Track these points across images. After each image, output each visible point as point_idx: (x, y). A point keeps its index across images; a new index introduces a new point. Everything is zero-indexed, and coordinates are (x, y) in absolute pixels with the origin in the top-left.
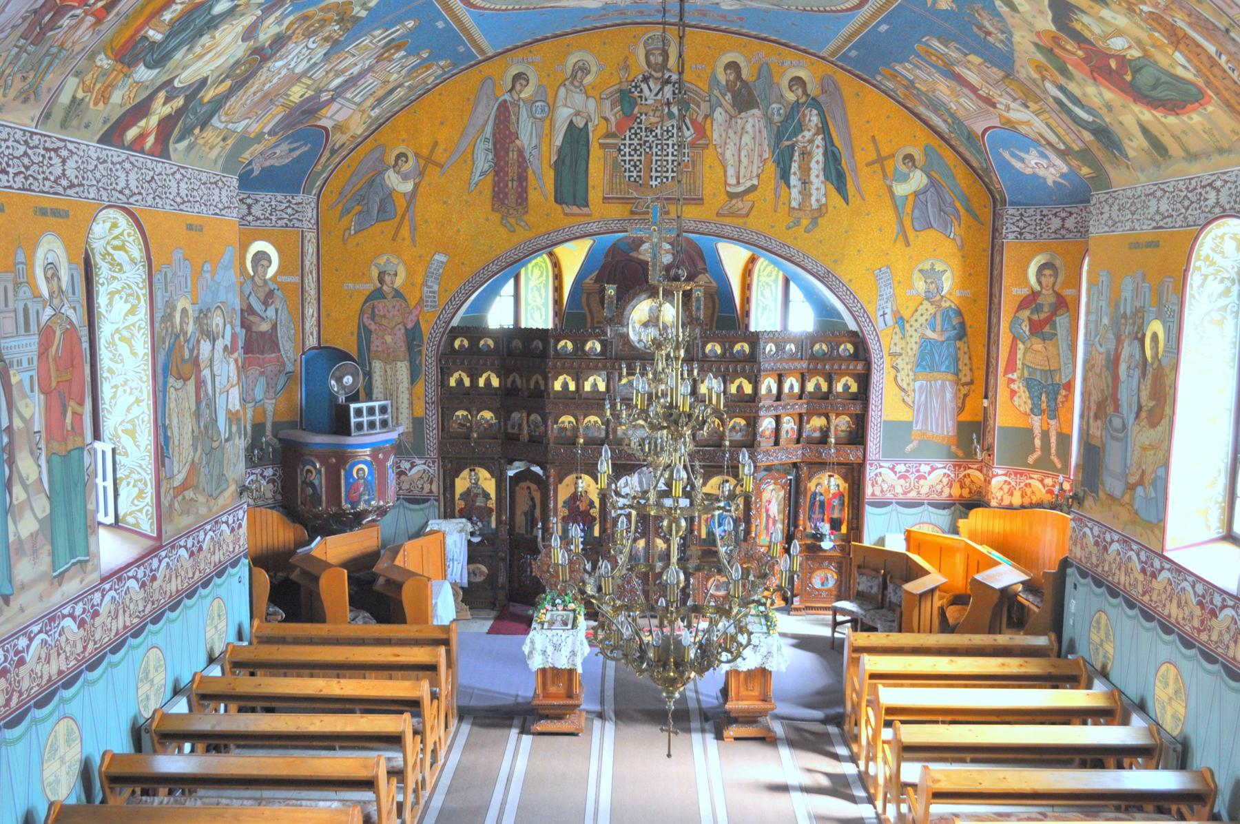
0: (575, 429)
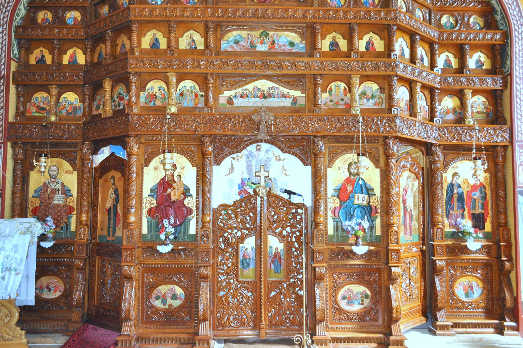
0: (167, 96)
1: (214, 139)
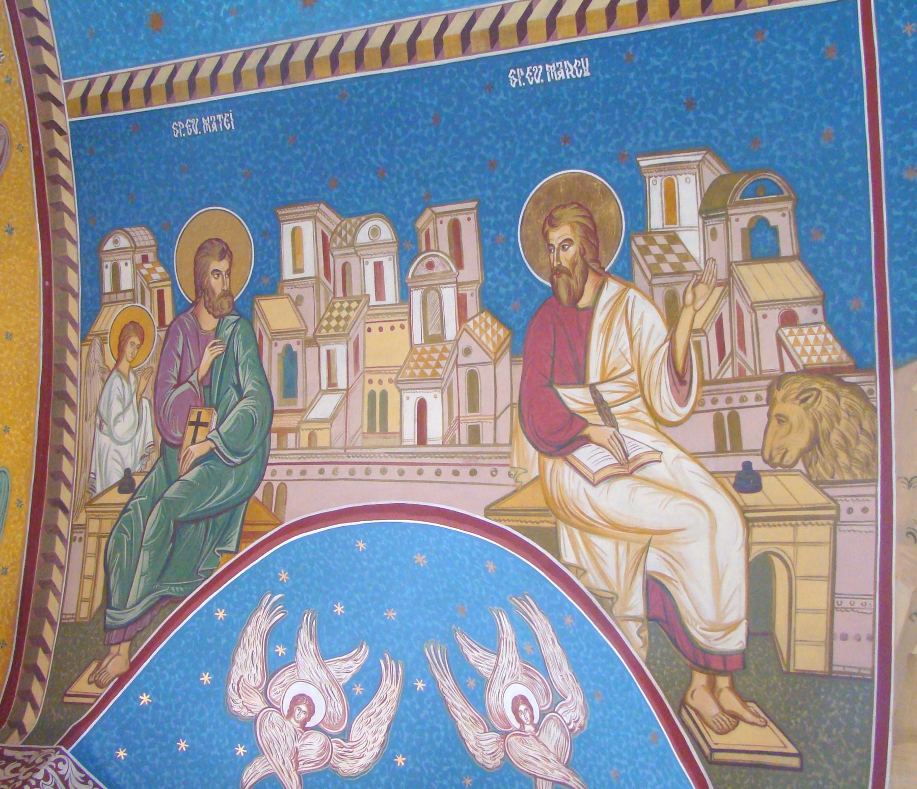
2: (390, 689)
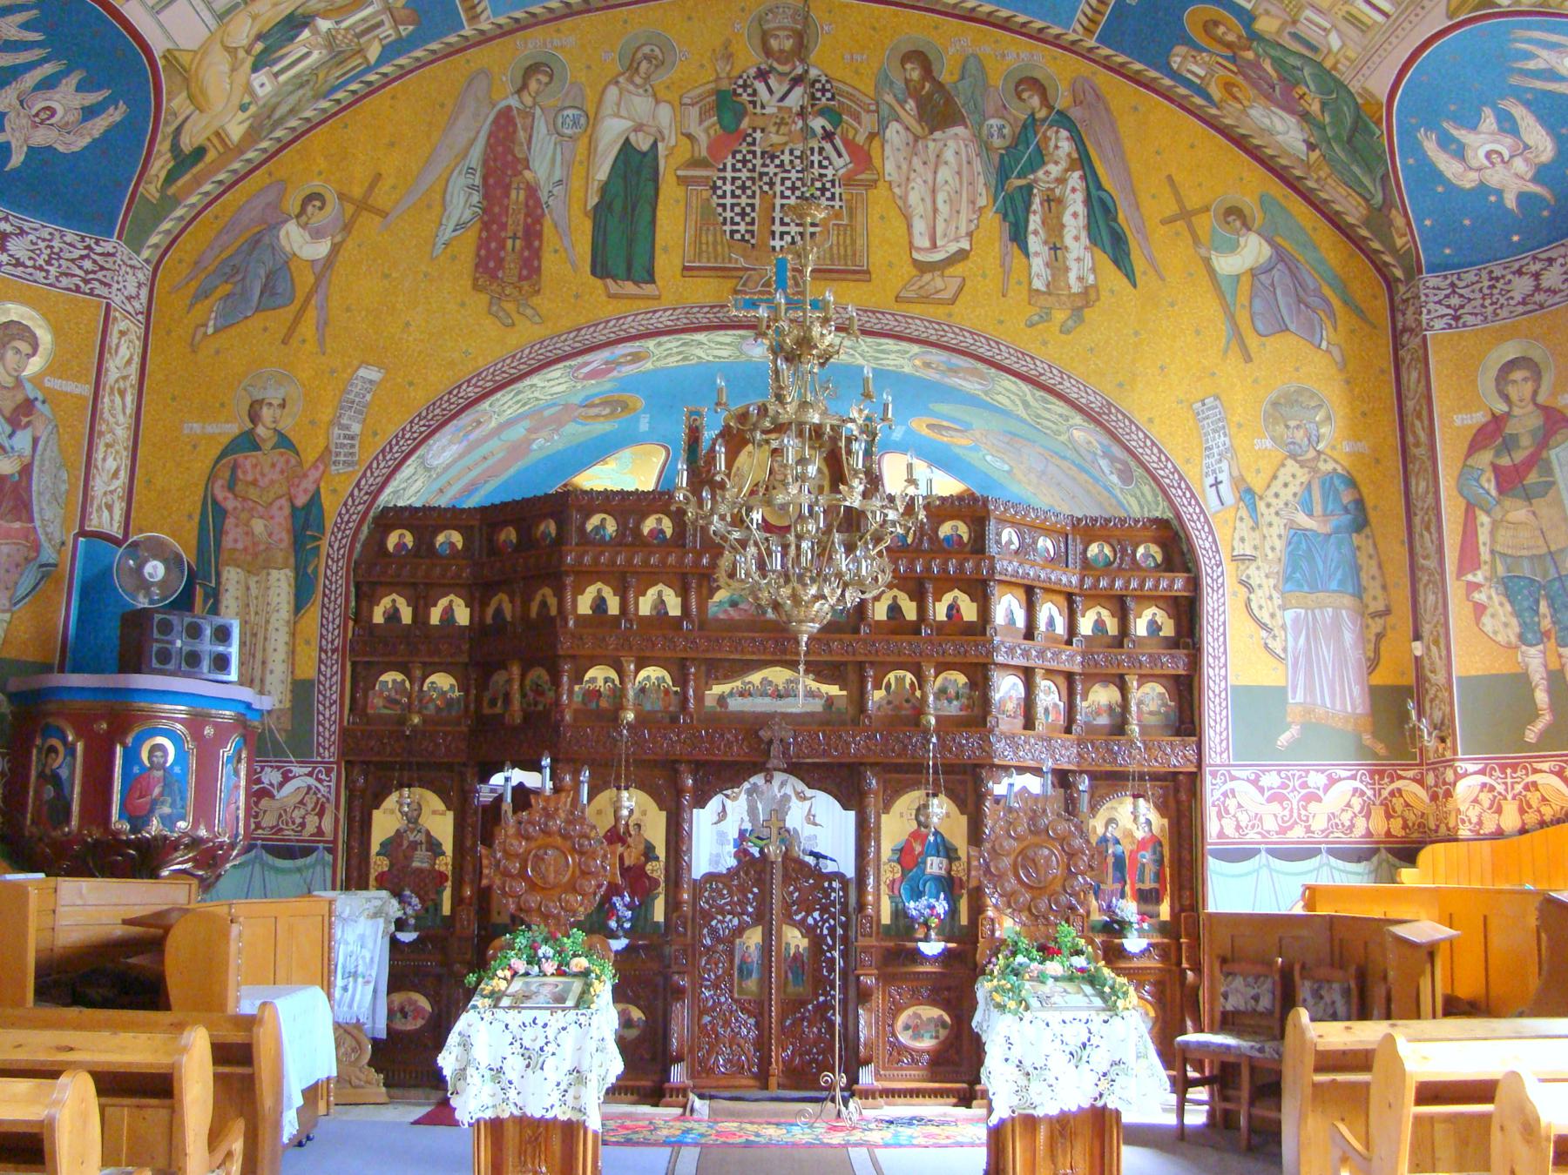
0: (618, 694)
1: (697, 766)
2: (1519, 112)
